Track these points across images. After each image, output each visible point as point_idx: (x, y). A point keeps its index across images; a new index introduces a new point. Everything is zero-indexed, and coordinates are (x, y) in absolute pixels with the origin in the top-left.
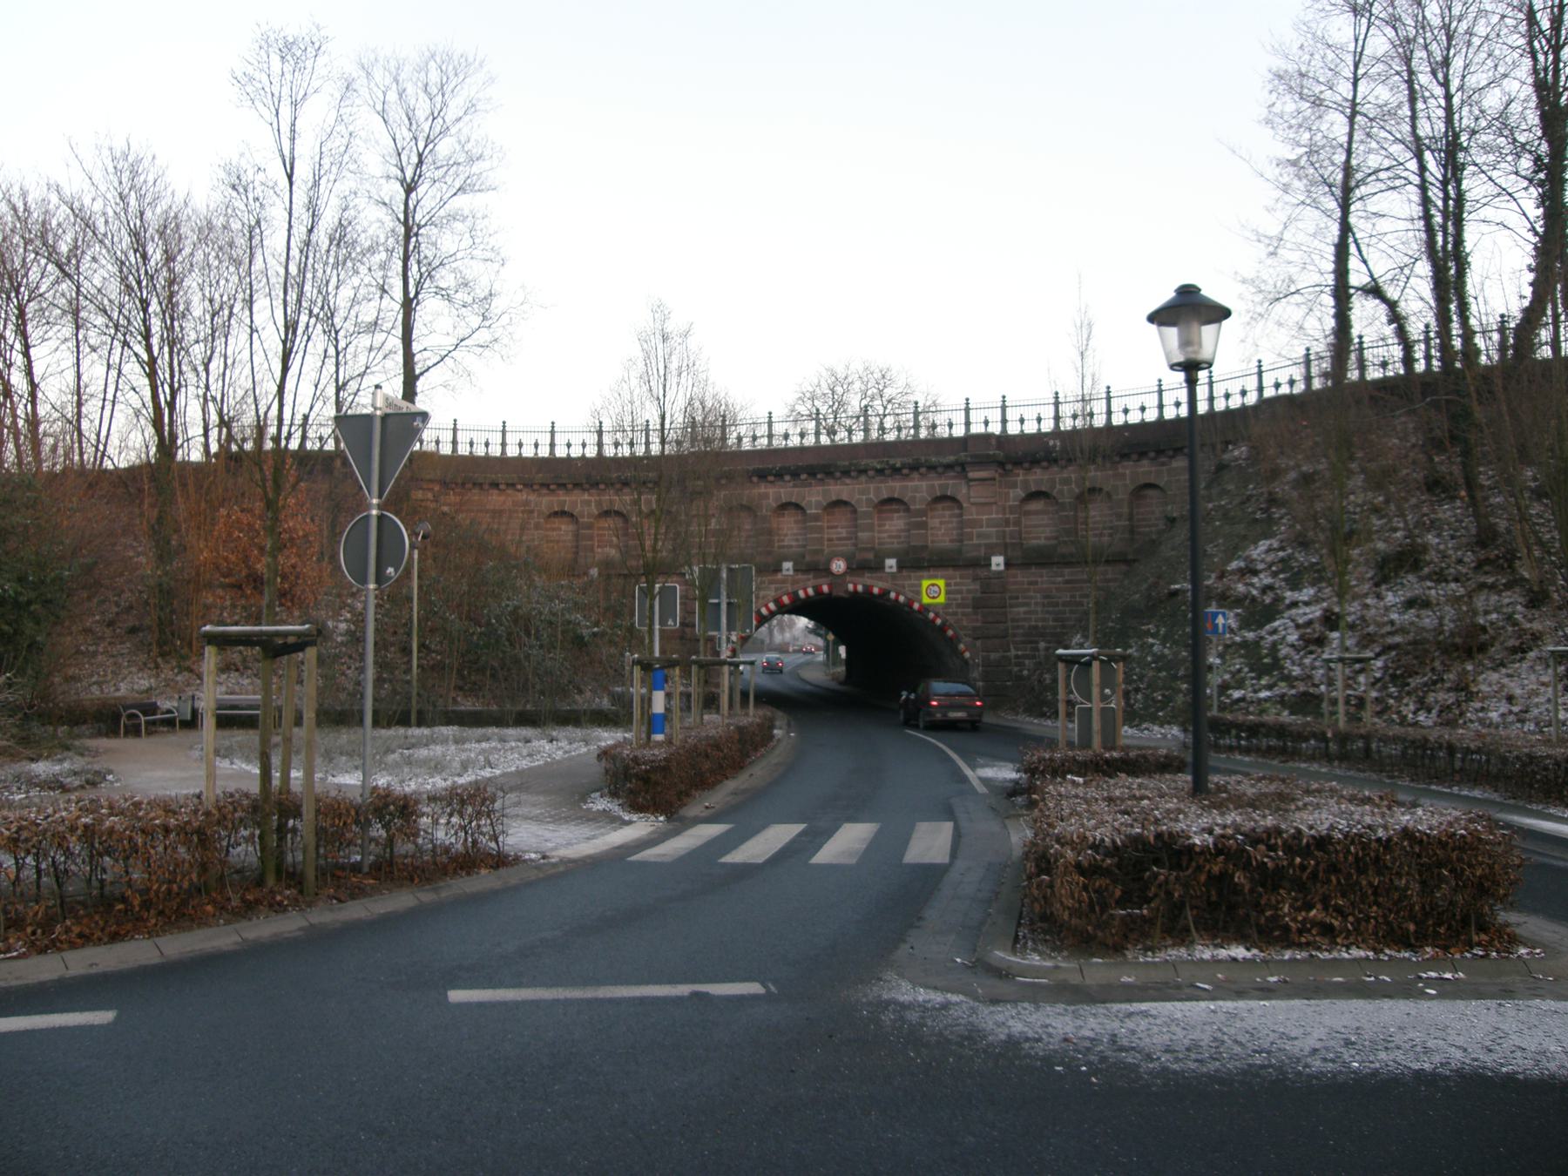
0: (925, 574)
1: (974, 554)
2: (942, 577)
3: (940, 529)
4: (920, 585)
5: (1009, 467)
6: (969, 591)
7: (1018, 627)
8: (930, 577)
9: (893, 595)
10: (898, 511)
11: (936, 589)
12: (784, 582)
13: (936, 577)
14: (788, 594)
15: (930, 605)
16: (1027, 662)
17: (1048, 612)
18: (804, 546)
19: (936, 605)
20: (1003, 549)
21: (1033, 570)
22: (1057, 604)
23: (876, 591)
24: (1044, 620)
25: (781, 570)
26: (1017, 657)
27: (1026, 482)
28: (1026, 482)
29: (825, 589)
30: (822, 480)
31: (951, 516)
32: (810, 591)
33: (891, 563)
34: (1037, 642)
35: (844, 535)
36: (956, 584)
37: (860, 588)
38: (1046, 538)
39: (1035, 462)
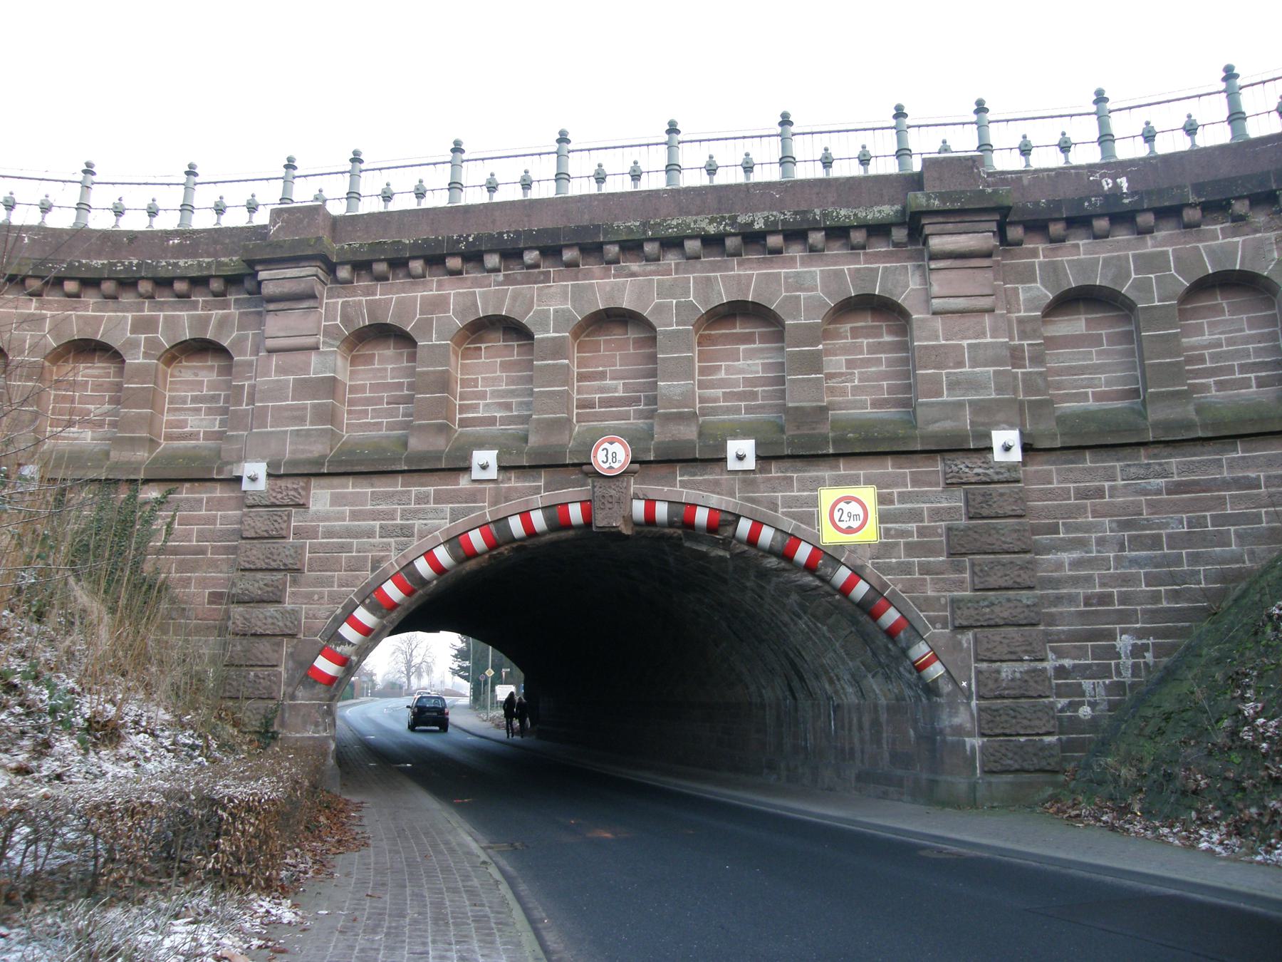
0: (827, 474)
1: (947, 425)
2: (868, 482)
3: (848, 377)
4: (815, 502)
5: (1015, 233)
6: (936, 514)
7: (1058, 600)
8: (838, 482)
9: (744, 527)
10: (748, 339)
11: (854, 508)
12: (473, 497)
13: (854, 481)
14: (483, 527)
15: (841, 548)
16: (1087, 684)
17: (1134, 562)
18: (526, 419)
19: (854, 548)
20: (1013, 412)
21: (1089, 461)
22: (1155, 542)
23: (702, 516)
24: (1125, 580)
25: (468, 469)
26: (1061, 671)
27: (1053, 270)
28: (1053, 270)
29: (575, 513)
30: (572, 264)
31: (874, 349)
32: (538, 520)
33: (741, 451)
34: (1111, 635)
35: (620, 394)
36: (903, 497)
37: (662, 511)
38: (1099, 397)
39: (1079, 222)
